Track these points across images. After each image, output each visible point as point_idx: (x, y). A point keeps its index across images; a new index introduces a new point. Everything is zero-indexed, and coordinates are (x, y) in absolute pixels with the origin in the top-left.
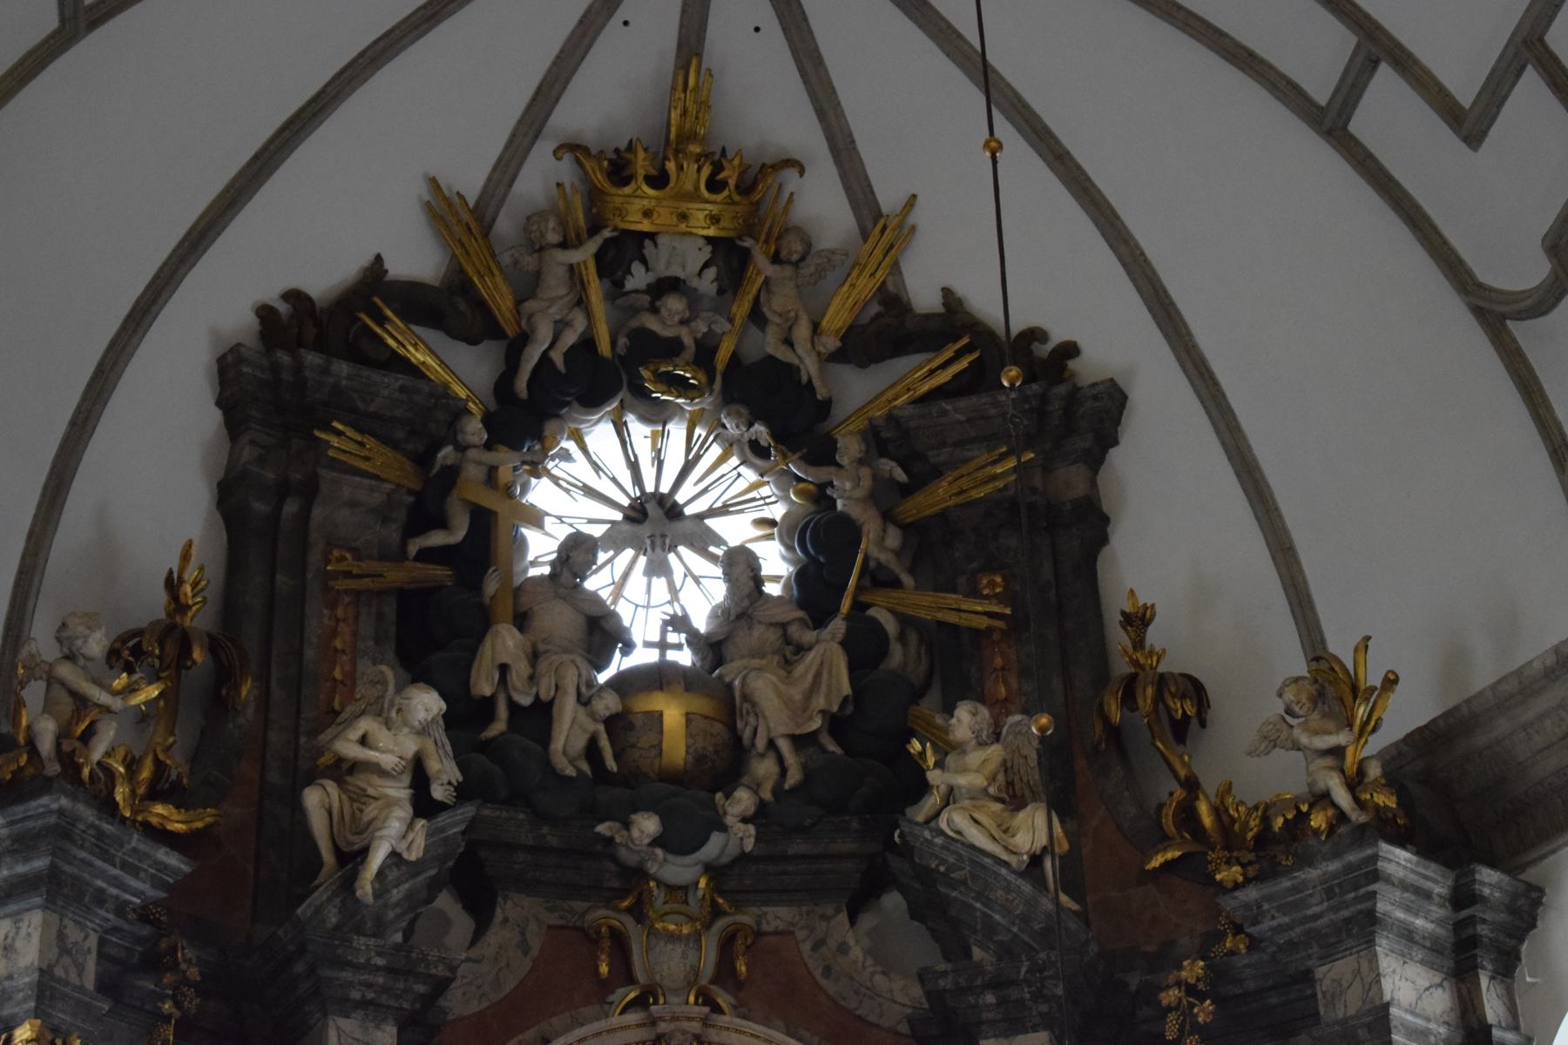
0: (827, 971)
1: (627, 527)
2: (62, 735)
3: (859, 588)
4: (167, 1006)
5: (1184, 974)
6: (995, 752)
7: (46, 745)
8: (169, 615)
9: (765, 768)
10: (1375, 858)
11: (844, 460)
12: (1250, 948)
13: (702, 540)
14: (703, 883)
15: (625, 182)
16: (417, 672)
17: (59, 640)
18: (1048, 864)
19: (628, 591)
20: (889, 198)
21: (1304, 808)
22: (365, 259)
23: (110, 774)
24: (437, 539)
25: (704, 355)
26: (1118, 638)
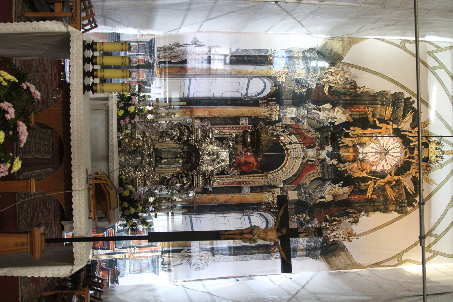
18: (323, 200)
24: (377, 122)
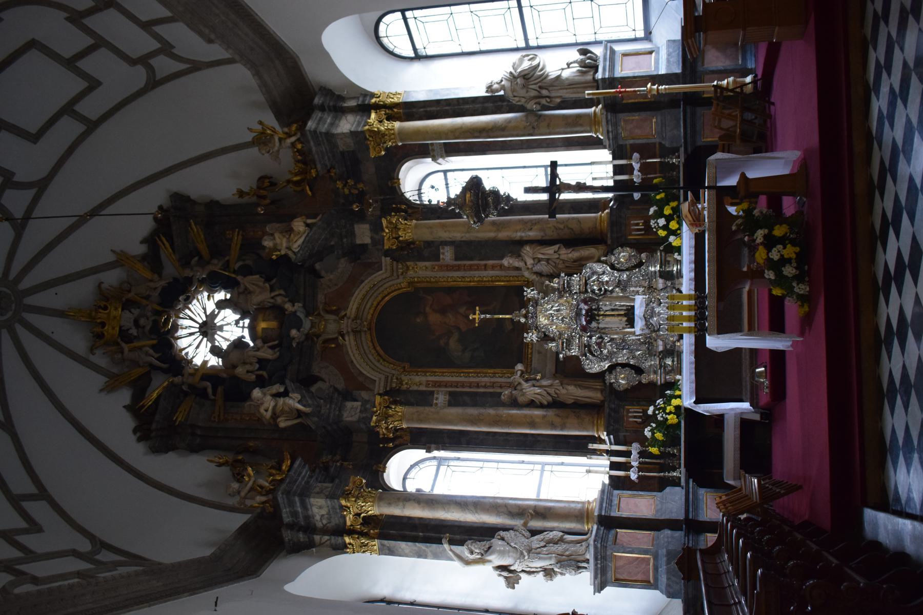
0: (336, 285)
1: (209, 337)
2: (261, 494)
3: (229, 272)
4: (338, 464)
5: (340, 187)
6: (277, 235)
7: (264, 499)
8: (228, 466)
9: (279, 300)
10: (310, 131)
11: (191, 274)
12: (334, 169)
13: (213, 316)
14: (310, 318)
15: (103, 334)
16: (247, 397)
17: (234, 496)
18: (309, 221)
19: (227, 337)
20: (112, 258)
21: (296, 150)
22: (124, 410)
23: (273, 481)
24: (210, 390)
25: (159, 314)
26: (246, 199)
